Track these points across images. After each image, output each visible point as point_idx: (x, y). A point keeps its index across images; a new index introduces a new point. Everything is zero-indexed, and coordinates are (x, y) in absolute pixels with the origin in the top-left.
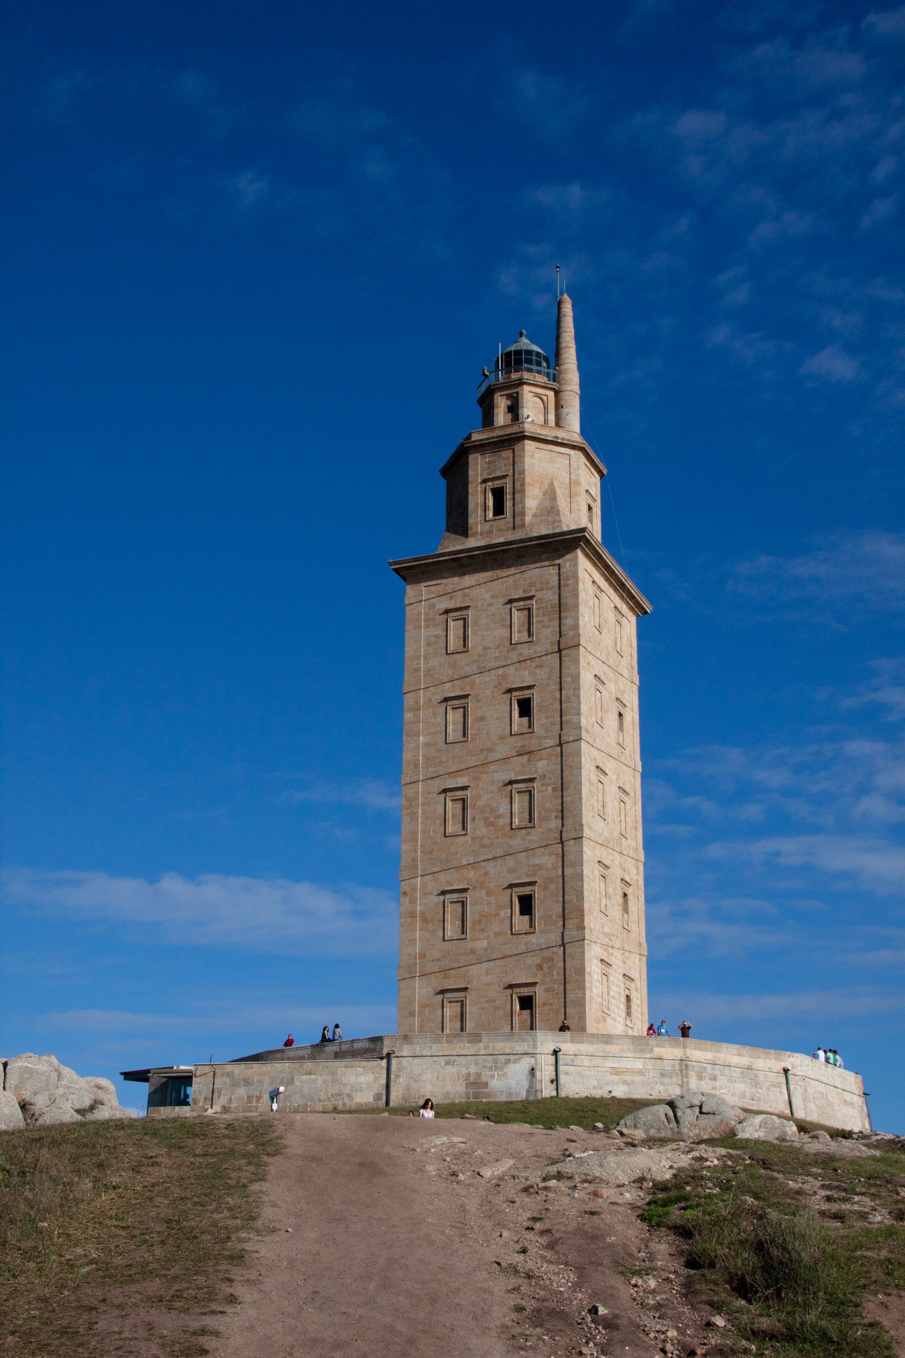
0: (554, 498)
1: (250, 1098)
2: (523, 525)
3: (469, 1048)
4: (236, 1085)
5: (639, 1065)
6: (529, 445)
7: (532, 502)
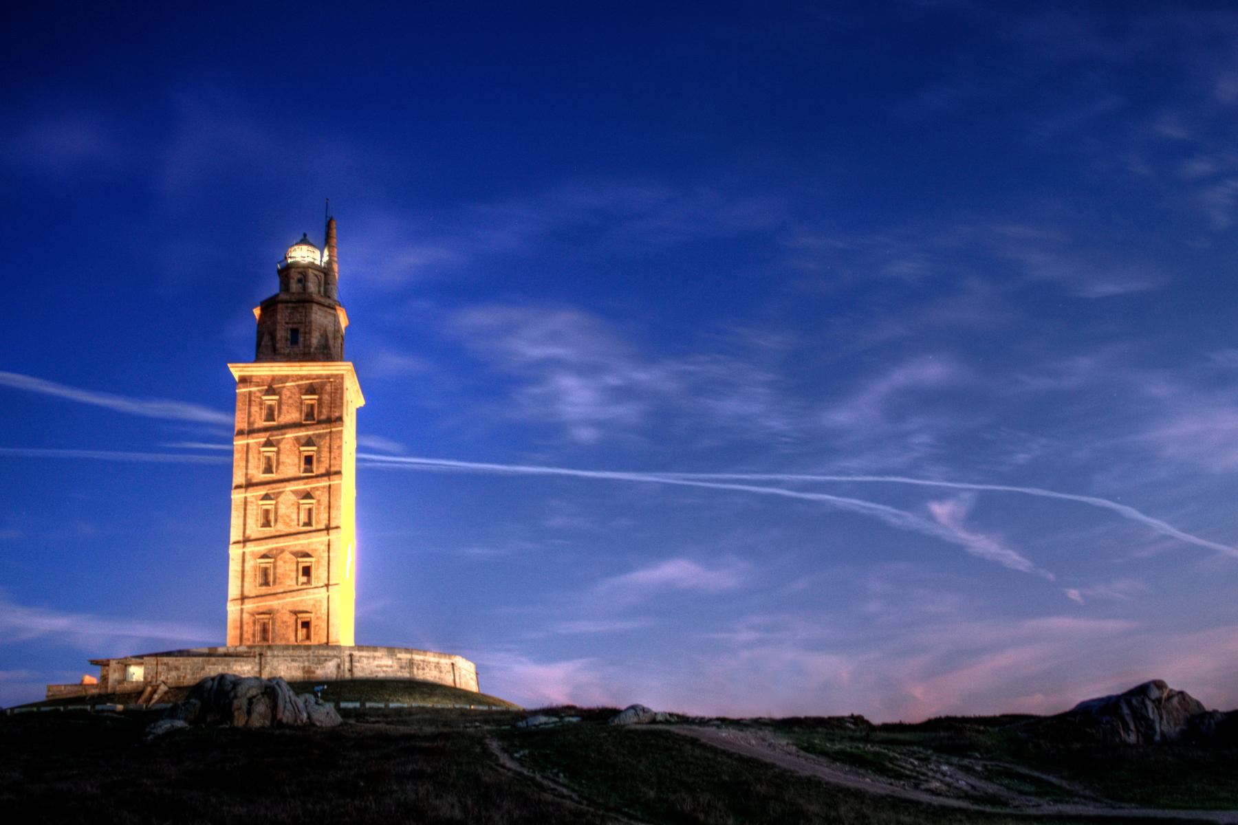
0: (327, 340)
1: (179, 677)
2: (309, 353)
3: (304, 653)
4: (170, 670)
5: (390, 663)
6: (315, 307)
7: (315, 341)
